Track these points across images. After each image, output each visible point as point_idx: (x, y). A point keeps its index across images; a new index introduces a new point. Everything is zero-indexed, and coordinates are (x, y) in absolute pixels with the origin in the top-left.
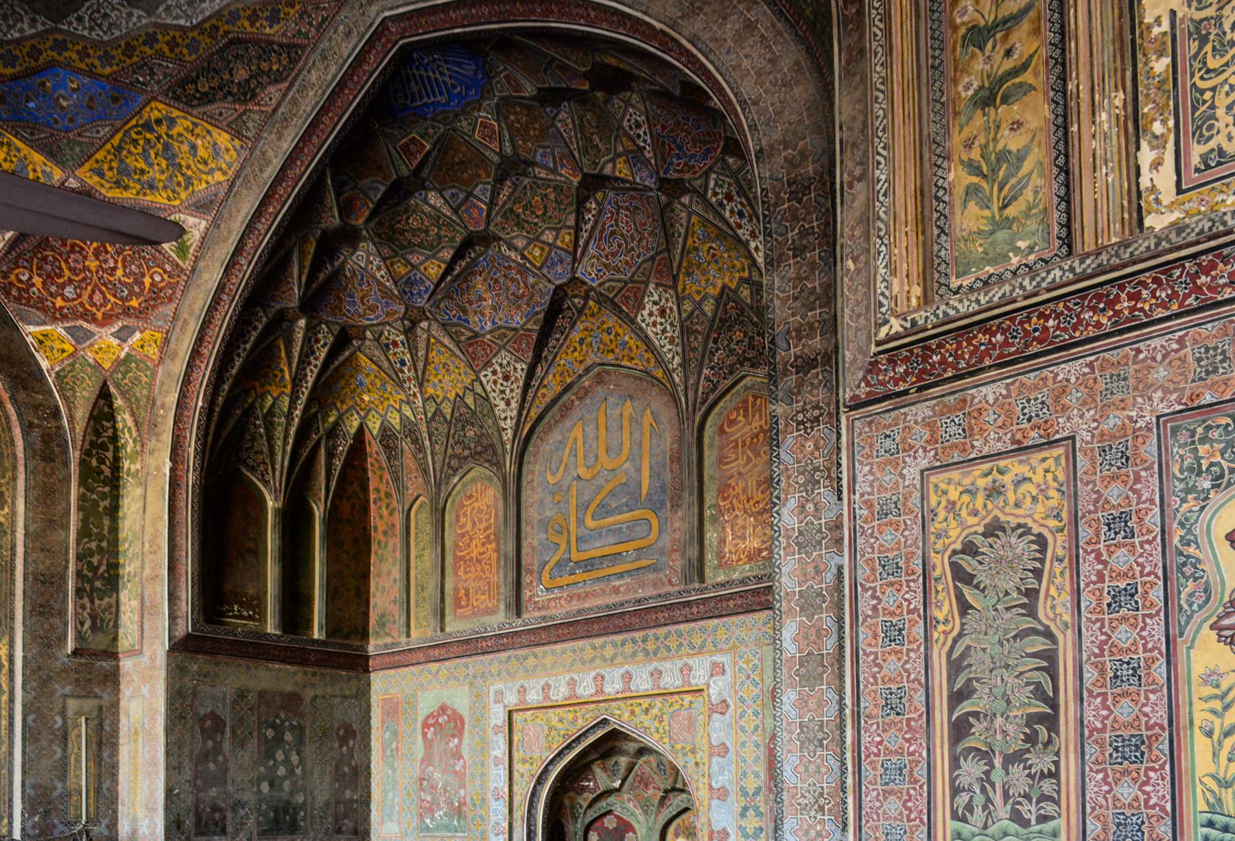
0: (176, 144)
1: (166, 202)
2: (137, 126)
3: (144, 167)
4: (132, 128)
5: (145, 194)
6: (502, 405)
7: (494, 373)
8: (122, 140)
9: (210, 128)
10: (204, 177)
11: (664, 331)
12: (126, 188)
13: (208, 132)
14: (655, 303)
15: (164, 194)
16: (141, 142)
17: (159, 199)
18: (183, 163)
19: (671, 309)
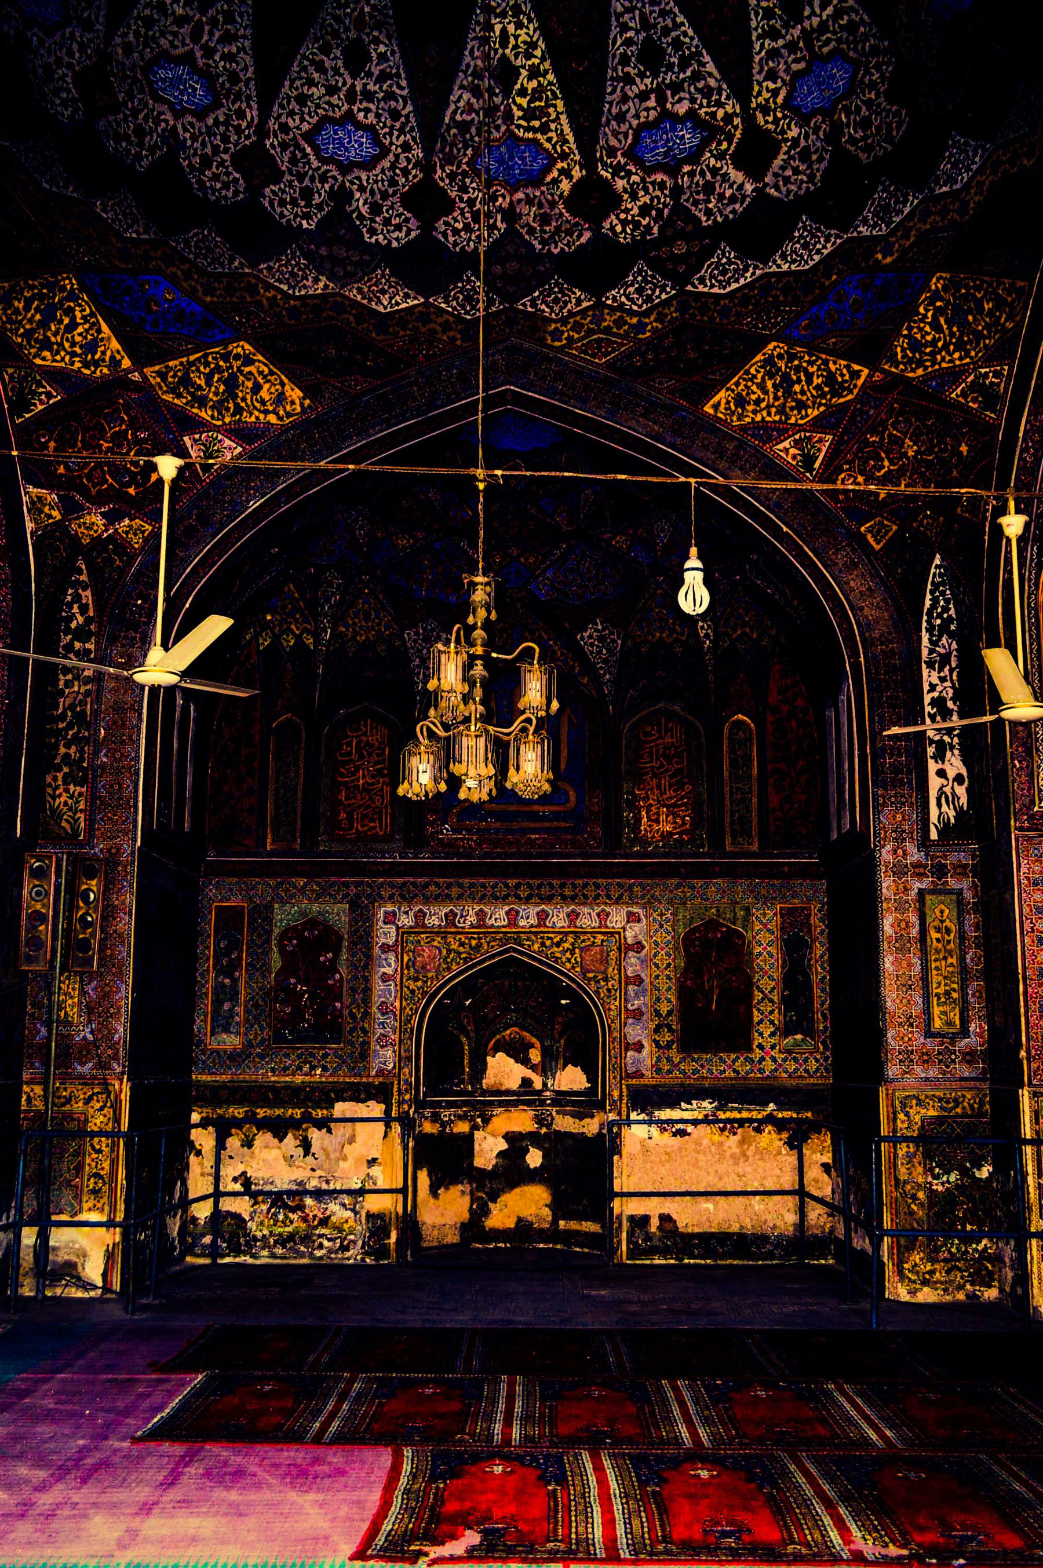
0: (241, 378)
1: (209, 419)
2: (216, 353)
3: (203, 384)
4: (212, 353)
5: (193, 407)
6: (417, 662)
7: (417, 634)
8: (198, 359)
9: (286, 380)
10: (257, 413)
11: (600, 652)
12: (179, 396)
13: (283, 384)
14: (596, 630)
15: (210, 413)
16: (212, 366)
17: (203, 414)
18: (240, 395)
19: (613, 641)
